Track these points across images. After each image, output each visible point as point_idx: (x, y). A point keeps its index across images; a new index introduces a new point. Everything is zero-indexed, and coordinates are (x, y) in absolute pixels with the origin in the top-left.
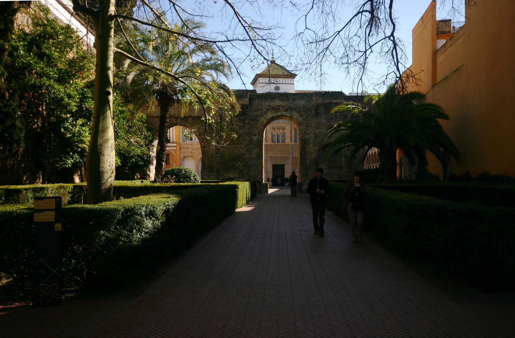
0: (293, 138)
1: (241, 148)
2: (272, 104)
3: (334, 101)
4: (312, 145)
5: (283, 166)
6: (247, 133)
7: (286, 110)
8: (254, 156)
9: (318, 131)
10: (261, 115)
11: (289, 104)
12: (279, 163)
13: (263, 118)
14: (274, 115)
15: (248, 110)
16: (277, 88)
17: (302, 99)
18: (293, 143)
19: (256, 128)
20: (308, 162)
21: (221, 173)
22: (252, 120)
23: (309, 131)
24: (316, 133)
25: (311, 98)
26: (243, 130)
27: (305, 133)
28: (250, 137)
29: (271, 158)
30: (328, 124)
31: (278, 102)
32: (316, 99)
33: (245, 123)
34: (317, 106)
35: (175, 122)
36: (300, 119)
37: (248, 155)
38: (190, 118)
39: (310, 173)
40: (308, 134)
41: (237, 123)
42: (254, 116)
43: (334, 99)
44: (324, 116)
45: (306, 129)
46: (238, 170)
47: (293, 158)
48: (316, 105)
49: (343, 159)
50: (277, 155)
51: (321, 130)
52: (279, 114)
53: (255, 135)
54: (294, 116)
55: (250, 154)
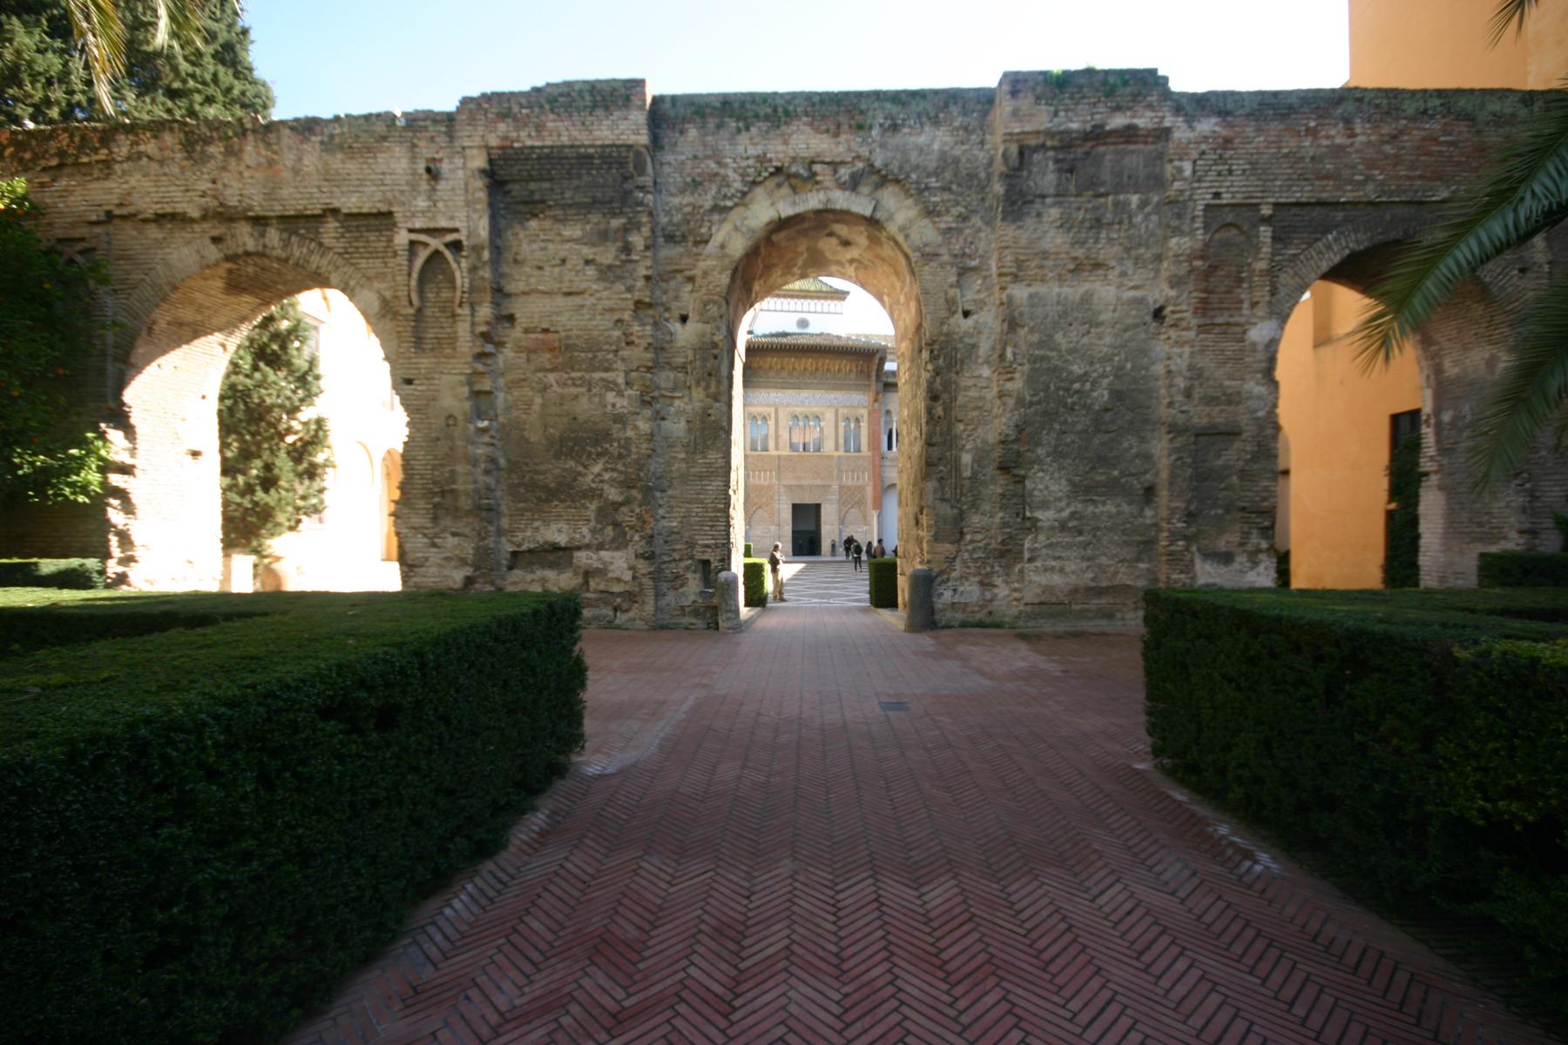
0: (841, 441)
1: (610, 386)
2: (778, 151)
3: (1118, 121)
4: (986, 372)
5: (818, 506)
6: (639, 304)
7: (853, 184)
8: (677, 428)
9: (1020, 293)
10: (716, 208)
11: (864, 152)
12: (808, 499)
13: (727, 227)
14: (786, 210)
15: (647, 180)
16: (803, 323)
17: (936, 122)
18: (841, 453)
19: (691, 279)
20: (966, 458)
21: (505, 522)
22: (670, 239)
23: (970, 295)
24: (1009, 303)
25: (985, 113)
26: (620, 287)
27: (951, 304)
28: (656, 324)
29: (789, 487)
30: (1079, 252)
31: (805, 141)
32: (1015, 113)
33: (627, 249)
34: (1021, 153)
35: (251, 245)
36: (925, 232)
37: (644, 426)
38: (331, 225)
39: (975, 519)
40: (966, 314)
41: (586, 251)
42: (677, 218)
43: (1118, 109)
44: (1054, 212)
45: (958, 284)
46: (593, 506)
47: (841, 487)
48: (1014, 149)
49: (1160, 447)
50: (804, 482)
51: (1037, 288)
52: (813, 201)
53: (684, 319)
54: (891, 217)
55: (659, 417)
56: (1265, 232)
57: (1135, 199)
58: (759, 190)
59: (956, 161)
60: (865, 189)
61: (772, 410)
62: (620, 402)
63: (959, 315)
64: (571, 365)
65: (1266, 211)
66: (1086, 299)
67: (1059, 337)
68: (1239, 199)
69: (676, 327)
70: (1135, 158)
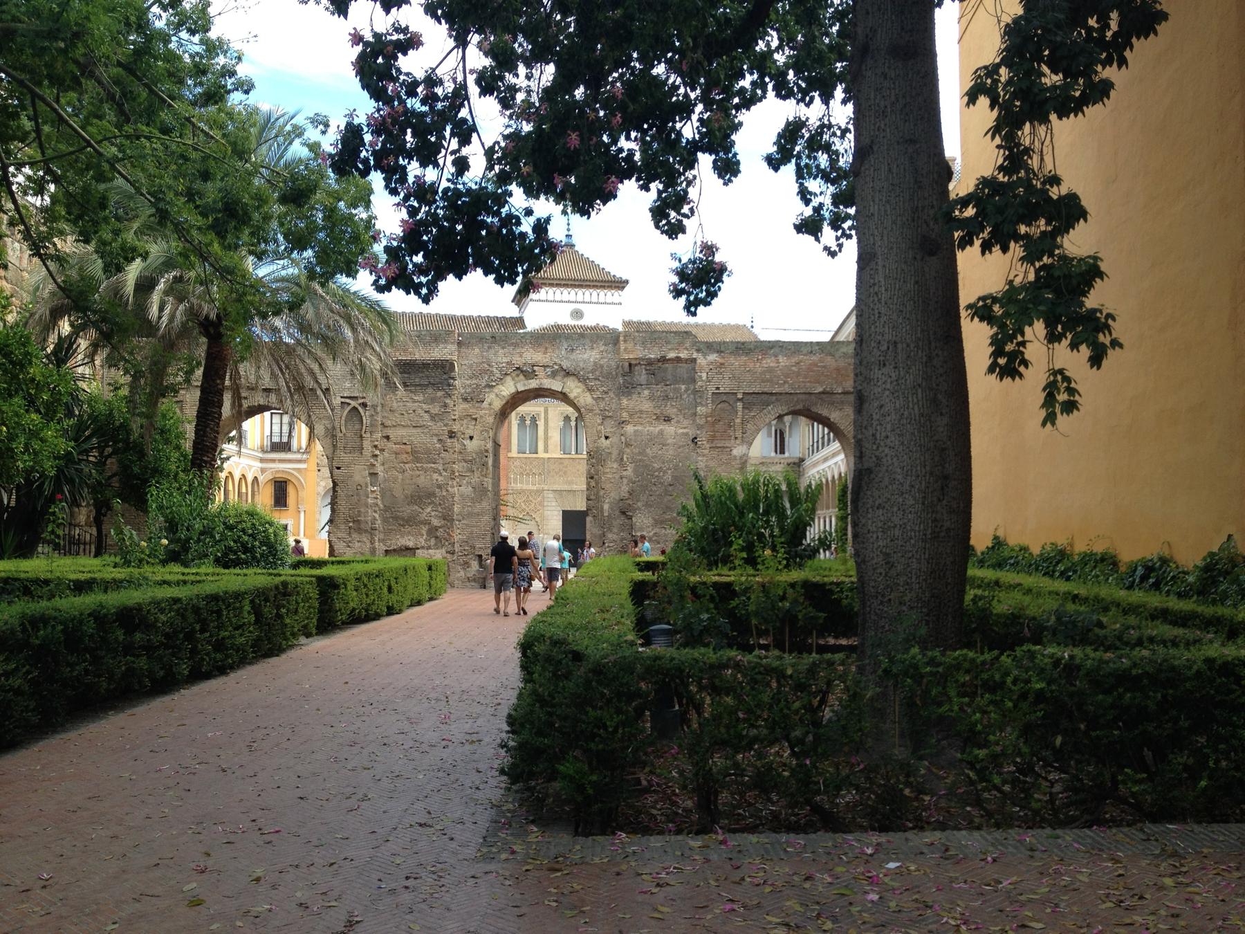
13: (492, 396)
16: (578, 314)
34: (630, 365)
40: (607, 438)
41: (424, 406)
52: (533, 384)
53: (471, 438)
56: (740, 405)
57: (683, 387)
58: (508, 378)
59: (602, 366)
60: (559, 378)
61: (542, 409)
62: (440, 478)
63: (603, 439)
64: (418, 460)
65: (740, 396)
66: (661, 433)
67: (648, 451)
68: (727, 390)
69: (467, 442)
70: (683, 369)
